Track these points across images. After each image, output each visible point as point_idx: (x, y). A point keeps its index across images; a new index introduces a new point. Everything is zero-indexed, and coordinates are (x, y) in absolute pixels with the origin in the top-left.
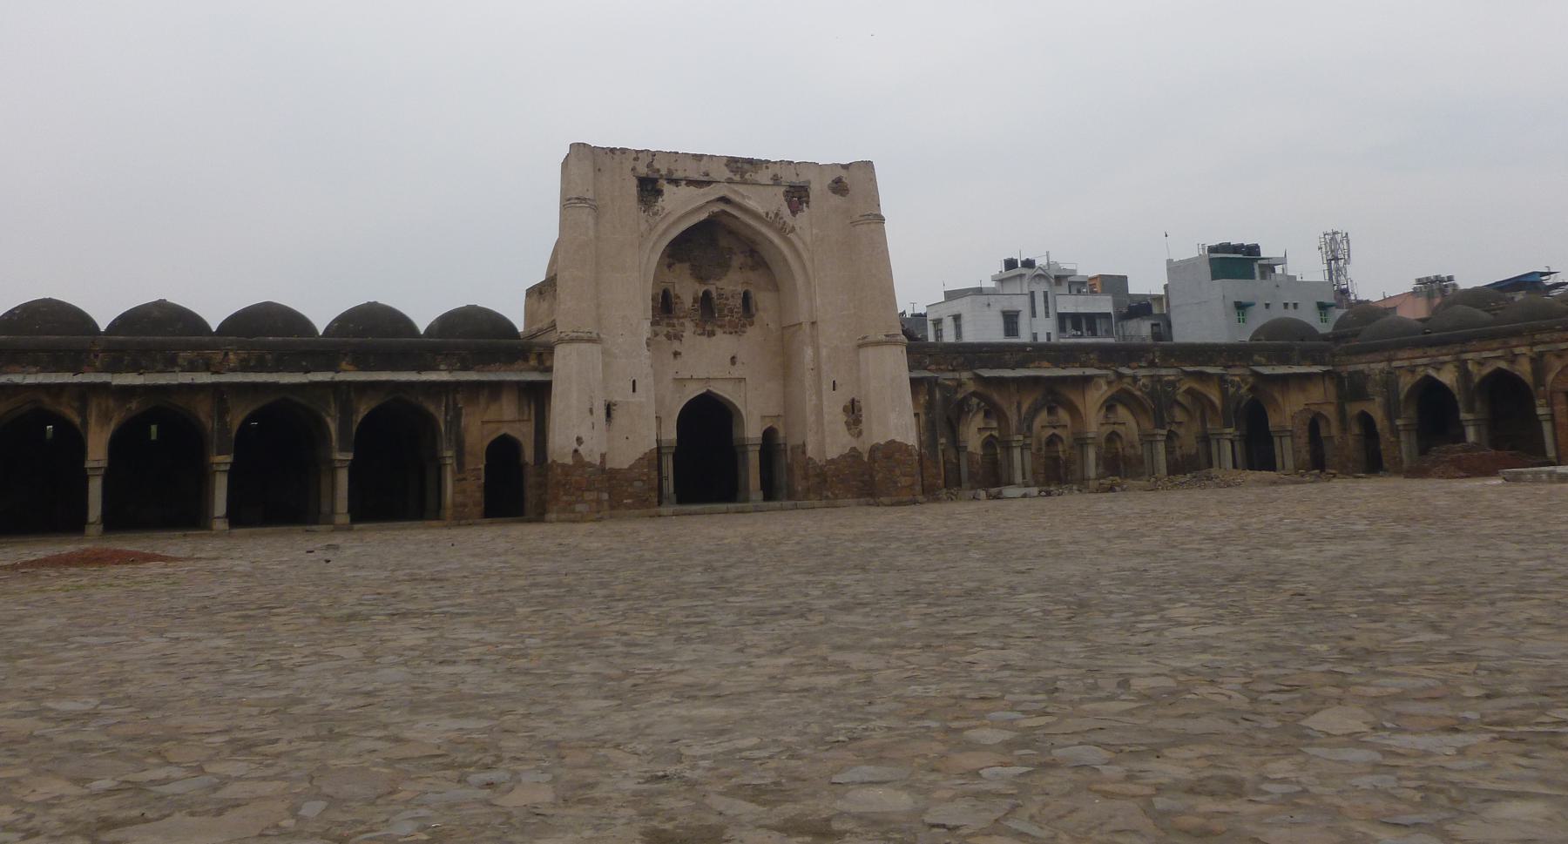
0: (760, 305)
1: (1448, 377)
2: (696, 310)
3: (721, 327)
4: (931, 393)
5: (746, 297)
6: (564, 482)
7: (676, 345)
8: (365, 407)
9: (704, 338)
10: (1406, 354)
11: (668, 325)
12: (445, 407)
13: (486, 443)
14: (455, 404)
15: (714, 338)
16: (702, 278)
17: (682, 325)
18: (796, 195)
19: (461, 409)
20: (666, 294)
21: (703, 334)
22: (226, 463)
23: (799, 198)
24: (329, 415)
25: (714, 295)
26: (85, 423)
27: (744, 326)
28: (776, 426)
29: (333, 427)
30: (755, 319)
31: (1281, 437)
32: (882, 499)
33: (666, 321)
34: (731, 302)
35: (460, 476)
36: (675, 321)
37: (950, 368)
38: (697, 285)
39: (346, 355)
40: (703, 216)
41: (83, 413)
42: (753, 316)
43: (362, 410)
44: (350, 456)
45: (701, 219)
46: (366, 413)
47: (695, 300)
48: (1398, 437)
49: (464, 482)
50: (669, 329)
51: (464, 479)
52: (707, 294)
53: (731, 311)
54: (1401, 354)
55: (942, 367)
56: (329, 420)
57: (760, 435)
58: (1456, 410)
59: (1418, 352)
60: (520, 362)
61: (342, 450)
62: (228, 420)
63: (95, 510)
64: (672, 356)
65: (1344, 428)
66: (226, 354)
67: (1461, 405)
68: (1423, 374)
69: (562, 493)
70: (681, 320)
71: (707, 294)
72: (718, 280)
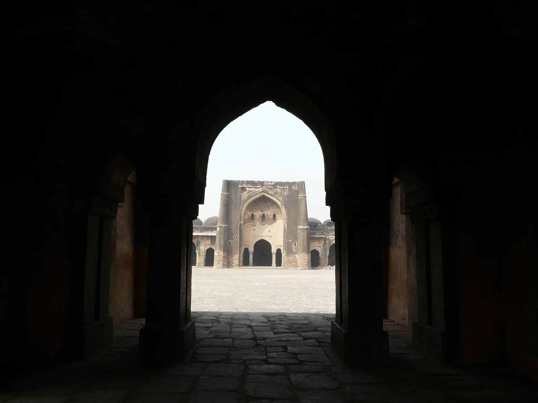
0: (277, 218)
2: (260, 219)
3: (266, 223)
4: (325, 241)
5: (274, 215)
7: (254, 228)
9: (262, 226)
11: (252, 223)
13: (206, 249)
14: (199, 240)
15: (264, 226)
16: (262, 211)
17: (256, 222)
18: (284, 190)
19: (200, 241)
20: (253, 214)
21: (262, 225)
23: (284, 191)
25: (265, 215)
27: (273, 223)
28: (280, 248)
30: (276, 221)
32: (299, 268)
33: (252, 221)
34: (270, 217)
35: (199, 257)
36: (254, 222)
37: (332, 235)
38: (261, 213)
40: (258, 196)
42: (276, 220)
45: (258, 197)
47: (260, 216)
50: (253, 224)
52: (264, 215)
53: (270, 219)
55: (329, 234)
57: (276, 250)
60: (215, 231)
64: (253, 230)
70: (256, 221)
71: (264, 215)
72: (266, 211)
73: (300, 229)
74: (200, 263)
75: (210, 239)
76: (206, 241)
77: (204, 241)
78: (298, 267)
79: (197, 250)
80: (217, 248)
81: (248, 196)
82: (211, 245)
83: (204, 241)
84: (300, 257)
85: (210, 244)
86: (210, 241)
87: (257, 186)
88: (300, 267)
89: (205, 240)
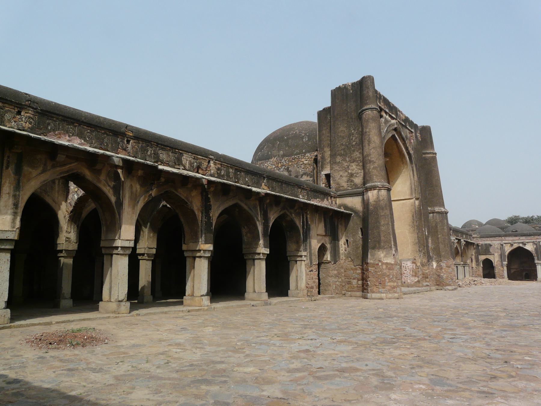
1: (529, 247)
6: (388, 274)
8: (273, 217)
10: (511, 238)
12: (303, 223)
22: (209, 251)
24: (258, 220)
26: (120, 204)
29: (260, 228)
31: (464, 267)
39: (264, 178)
41: (118, 189)
43: (271, 219)
44: (267, 251)
46: (273, 221)
48: (503, 268)
49: (312, 272)
51: (312, 271)
54: (507, 238)
56: (258, 223)
58: (533, 259)
59: (517, 238)
61: (265, 247)
62: (211, 215)
63: (66, 287)
65: (478, 265)
66: (209, 162)
67: (536, 258)
68: (517, 246)
69: (387, 281)
73: (437, 212)
74: (312, 288)
75: (323, 219)
76: (318, 224)
77: (315, 223)
78: (446, 286)
79: (305, 250)
80: (390, 243)
81: (387, 130)
82: (324, 237)
83: (315, 225)
84: (447, 267)
85: (324, 234)
86: (323, 224)
87: (392, 114)
88: (450, 285)
89: (317, 222)
